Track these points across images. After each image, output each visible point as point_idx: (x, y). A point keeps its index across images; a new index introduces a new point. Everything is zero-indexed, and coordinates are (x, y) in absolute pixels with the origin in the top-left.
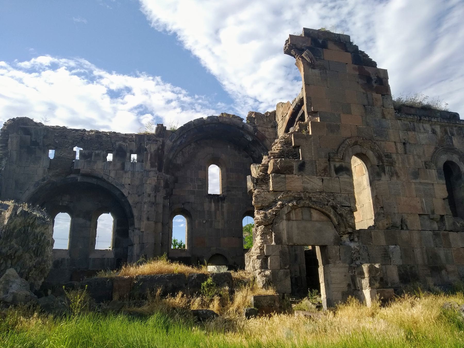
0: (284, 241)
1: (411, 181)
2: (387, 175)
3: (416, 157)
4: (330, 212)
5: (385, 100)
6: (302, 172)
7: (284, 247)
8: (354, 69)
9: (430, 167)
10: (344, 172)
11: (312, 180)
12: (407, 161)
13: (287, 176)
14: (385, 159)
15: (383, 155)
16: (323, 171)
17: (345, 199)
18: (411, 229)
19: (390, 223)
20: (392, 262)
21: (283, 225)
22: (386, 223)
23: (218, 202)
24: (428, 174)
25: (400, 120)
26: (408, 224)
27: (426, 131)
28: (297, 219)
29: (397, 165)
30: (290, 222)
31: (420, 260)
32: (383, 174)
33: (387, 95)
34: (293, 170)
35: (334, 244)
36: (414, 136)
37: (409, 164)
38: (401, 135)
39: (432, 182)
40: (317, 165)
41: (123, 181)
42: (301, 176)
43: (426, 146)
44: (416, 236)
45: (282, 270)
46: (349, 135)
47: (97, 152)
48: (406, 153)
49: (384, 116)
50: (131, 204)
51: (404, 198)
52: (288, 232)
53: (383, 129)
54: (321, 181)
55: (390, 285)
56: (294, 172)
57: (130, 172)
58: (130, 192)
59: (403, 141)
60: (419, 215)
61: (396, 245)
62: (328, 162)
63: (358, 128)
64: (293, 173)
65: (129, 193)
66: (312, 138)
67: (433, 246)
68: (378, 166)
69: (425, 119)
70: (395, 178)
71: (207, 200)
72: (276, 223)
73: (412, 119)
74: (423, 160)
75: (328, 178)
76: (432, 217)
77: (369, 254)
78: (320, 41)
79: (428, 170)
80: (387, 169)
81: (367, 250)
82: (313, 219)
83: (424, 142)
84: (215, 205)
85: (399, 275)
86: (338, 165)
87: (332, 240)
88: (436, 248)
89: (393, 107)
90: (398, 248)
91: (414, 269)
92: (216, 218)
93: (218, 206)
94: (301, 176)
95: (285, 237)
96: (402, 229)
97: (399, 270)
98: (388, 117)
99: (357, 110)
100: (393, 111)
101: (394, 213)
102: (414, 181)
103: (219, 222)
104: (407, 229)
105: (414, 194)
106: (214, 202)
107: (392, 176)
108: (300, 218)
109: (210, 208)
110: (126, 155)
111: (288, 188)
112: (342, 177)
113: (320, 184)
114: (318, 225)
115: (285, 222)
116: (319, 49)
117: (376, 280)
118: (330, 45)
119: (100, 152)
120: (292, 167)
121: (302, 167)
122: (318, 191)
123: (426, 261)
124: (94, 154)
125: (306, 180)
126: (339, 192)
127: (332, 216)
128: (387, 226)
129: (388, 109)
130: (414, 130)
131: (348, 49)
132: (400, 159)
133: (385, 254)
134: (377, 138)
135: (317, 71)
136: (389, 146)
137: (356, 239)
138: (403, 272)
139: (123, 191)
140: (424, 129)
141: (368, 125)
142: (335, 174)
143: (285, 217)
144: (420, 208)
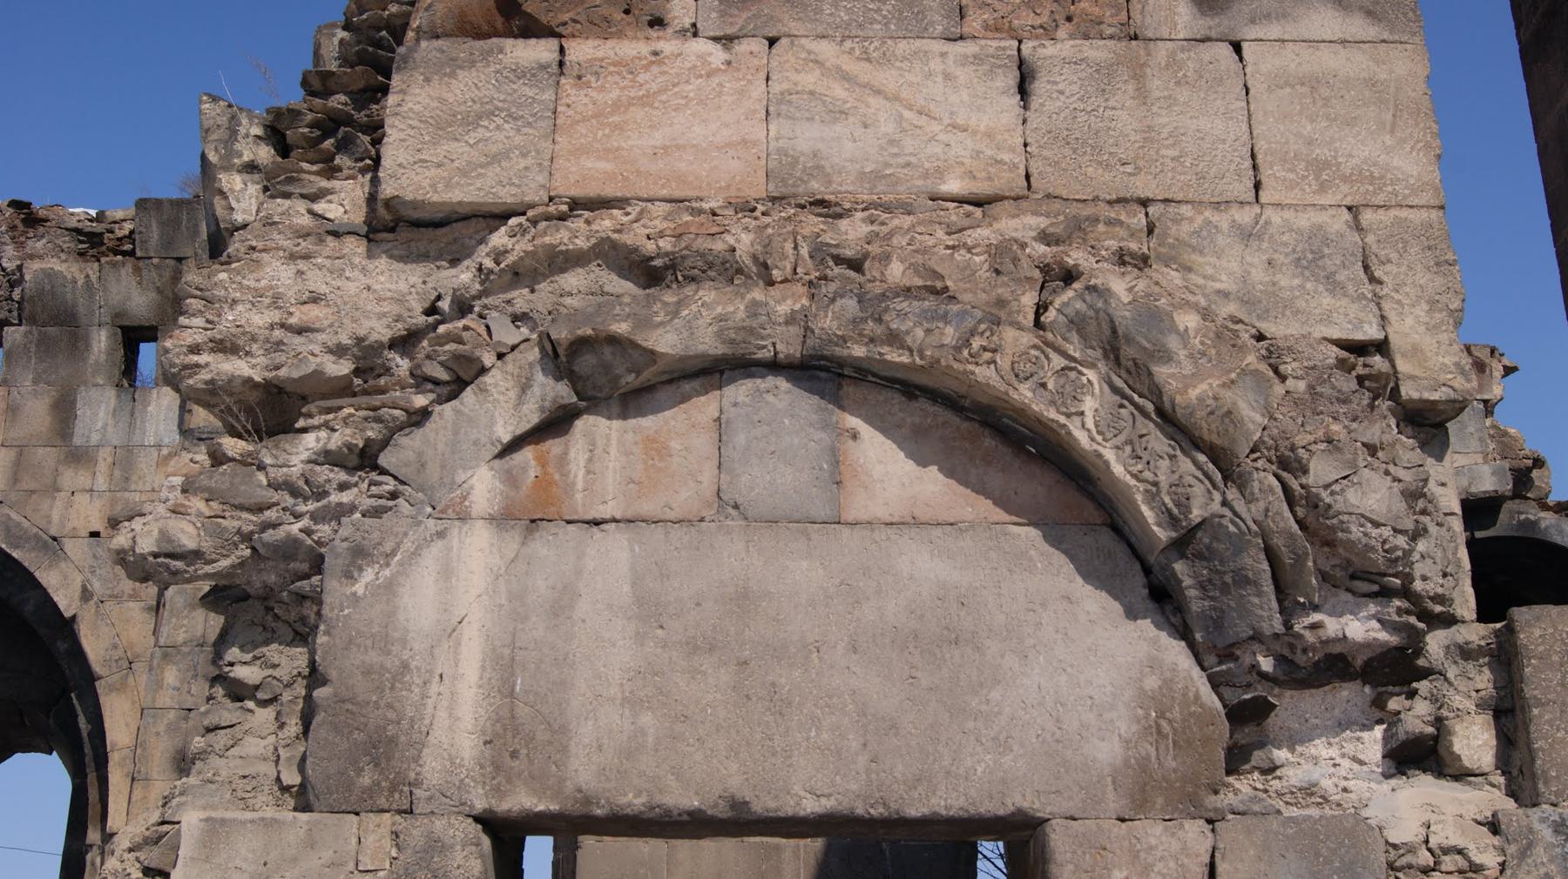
0: (432, 769)
4: (1069, 398)
7: (435, 846)
11: (887, 78)
13: (581, 50)
21: (447, 572)
28: (647, 508)
30: (552, 550)
35: (1137, 806)
41: (55, 517)
50: (97, 667)
52: (504, 669)
54: (1012, 78)
57: (105, 456)
58: (96, 586)
64: (657, 22)
65: (86, 595)
72: (360, 554)
75: (1098, 51)
82: (859, 506)
87: (1106, 751)
95: (453, 730)
108: (684, 498)
110: (88, 346)
111: (584, 172)
112: (1274, 31)
113: (983, 122)
114: (924, 566)
115: (477, 551)
122: (953, 186)
125: (809, 79)
139: (49, 578)
143: (483, 486)
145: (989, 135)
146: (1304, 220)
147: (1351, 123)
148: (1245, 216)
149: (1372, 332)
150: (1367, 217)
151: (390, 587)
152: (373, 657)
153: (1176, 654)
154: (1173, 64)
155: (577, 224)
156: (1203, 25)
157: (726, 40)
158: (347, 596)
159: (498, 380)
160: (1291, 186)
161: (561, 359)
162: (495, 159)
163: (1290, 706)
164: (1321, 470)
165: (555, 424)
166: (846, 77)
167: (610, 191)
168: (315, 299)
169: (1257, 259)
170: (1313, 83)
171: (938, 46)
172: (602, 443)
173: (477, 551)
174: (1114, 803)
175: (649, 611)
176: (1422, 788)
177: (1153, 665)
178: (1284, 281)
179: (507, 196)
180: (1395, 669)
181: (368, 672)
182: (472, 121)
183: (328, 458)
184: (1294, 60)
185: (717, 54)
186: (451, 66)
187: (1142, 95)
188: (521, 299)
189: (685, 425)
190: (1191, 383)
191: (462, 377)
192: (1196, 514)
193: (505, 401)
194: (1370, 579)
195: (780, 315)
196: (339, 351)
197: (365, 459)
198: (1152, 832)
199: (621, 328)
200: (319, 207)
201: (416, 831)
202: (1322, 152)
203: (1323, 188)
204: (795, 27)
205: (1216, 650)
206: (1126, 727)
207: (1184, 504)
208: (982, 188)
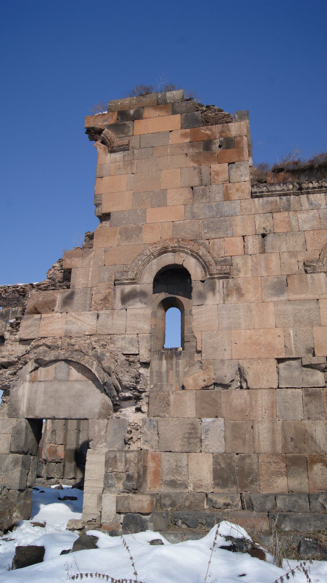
0: (21, 413)
1: (269, 300)
2: (217, 295)
3: (285, 255)
4: (92, 365)
5: (234, 170)
6: (67, 308)
7: (21, 422)
8: (184, 135)
9: (314, 269)
10: (137, 300)
11: (80, 318)
12: (263, 264)
13: (44, 316)
14: (215, 269)
15: (212, 262)
16: (100, 302)
17: (131, 342)
18: (254, 387)
19: (209, 379)
20: (203, 447)
21: (23, 388)
22: (202, 378)
23: (172, 358)
24: (310, 281)
25: (257, 197)
26: (250, 377)
27: (313, 206)
28: (46, 379)
29: (241, 275)
30: (35, 385)
31: (264, 443)
32: (210, 295)
33: (239, 161)
34: (54, 305)
36: (287, 220)
37: (268, 268)
38: (257, 223)
39: (317, 297)
40: (94, 292)
42: (64, 314)
43: (312, 232)
44: (263, 400)
45: (11, 455)
46: (157, 239)
47: (14, 309)
48: (263, 251)
49: (227, 197)
51: (248, 332)
52: (29, 400)
53: (222, 218)
54: (96, 317)
55: (190, 488)
56: (56, 309)
59: (262, 232)
60: (280, 361)
61: (217, 417)
62: (112, 287)
63: (174, 226)
64: (53, 311)
66: (92, 254)
67: (300, 417)
68: (203, 282)
69: (311, 185)
70: (233, 299)
71: (156, 356)
72: (14, 386)
73: (283, 190)
74: (301, 258)
75: (108, 312)
76: (305, 363)
77: (160, 433)
78: (132, 112)
79: (309, 276)
80: (219, 284)
81: (156, 427)
82: (71, 379)
83: (306, 227)
84: (167, 364)
85: (215, 471)
86: (128, 288)
87: (97, 410)
88: (306, 422)
89: (247, 179)
90: (220, 421)
91: (248, 461)
92: (167, 381)
93: (172, 364)
94: (64, 314)
95: (23, 407)
96: (241, 387)
97: (216, 462)
98: (235, 196)
99: (177, 198)
100: (247, 187)
101: (222, 361)
102: (275, 299)
103: (172, 385)
104: (248, 388)
105: (272, 321)
106: (166, 359)
107: (228, 295)
108: (50, 378)
109: (160, 367)
111: (43, 334)
112: (131, 307)
113: (91, 324)
114: (78, 386)
115: (27, 385)
116: (127, 122)
117: (119, 479)
118: (148, 113)
119: (17, 308)
120: (54, 302)
121: (68, 300)
122: (87, 333)
123: (279, 448)
124: (11, 312)
125: (71, 318)
126: (123, 332)
127: (93, 370)
128: (203, 384)
129: (237, 185)
130: (288, 208)
131: (178, 110)
132: (250, 264)
133: (190, 433)
134: (208, 236)
135: (118, 156)
136: (229, 246)
137: (145, 408)
138: (223, 465)
140: (311, 204)
141: (194, 216)
142: (120, 304)
144: (281, 346)
145: (92, 325)
146: (131, 336)
147: (140, 321)
148: (123, 336)
149: (137, 352)
150: (139, 335)
151: (17, 390)
152: (15, 399)
153: (107, 398)
154: (118, 313)
155: (41, 341)
156: (122, 307)
157: (61, 313)
158: (12, 391)
159: (30, 363)
160: (130, 331)
161: (37, 361)
162: (32, 332)
163: (124, 403)
164: (120, 375)
165: (36, 369)
166: (75, 318)
167: (45, 336)
168: (13, 351)
169: (124, 342)
170: (135, 315)
171: (87, 312)
172: (42, 370)
173: (27, 385)
174: (97, 417)
175: (46, 393)
176: (139, 414)
177: (103, 399)
178: (127, 345)
179: (33, 337)
180: (138, 398)
181: (15, 401)
182: (30, 327)
183: (10, 374)
184: (134, 312)
185: (60, 315)
186: (28, 318)
187: (113, 318)
188: (35, 351)
189: (51, 368)
190: (106, 364)
191: (26, 363)
192: (105, 381)
193: (30, 366)
194: (127, 388)
195: (62, 354)
196: (16, 357)
197: (15, 374)
198: (101, 421)
199: (41, 357)
200: (15, 336)
201: (19, 420)
202: (135, 326)
203: (134, 331)
204: (70, 311)
205: (112, 397)
206: (99, 407)
207: (104, 380)
208: (91, 333)
